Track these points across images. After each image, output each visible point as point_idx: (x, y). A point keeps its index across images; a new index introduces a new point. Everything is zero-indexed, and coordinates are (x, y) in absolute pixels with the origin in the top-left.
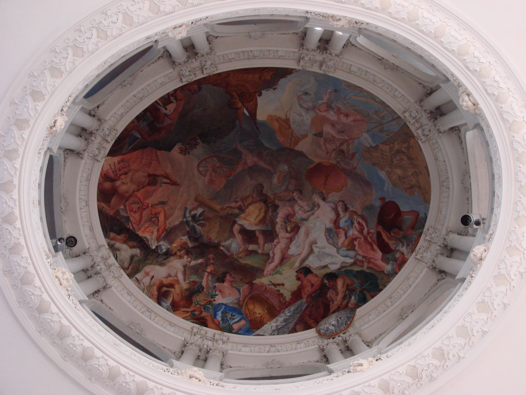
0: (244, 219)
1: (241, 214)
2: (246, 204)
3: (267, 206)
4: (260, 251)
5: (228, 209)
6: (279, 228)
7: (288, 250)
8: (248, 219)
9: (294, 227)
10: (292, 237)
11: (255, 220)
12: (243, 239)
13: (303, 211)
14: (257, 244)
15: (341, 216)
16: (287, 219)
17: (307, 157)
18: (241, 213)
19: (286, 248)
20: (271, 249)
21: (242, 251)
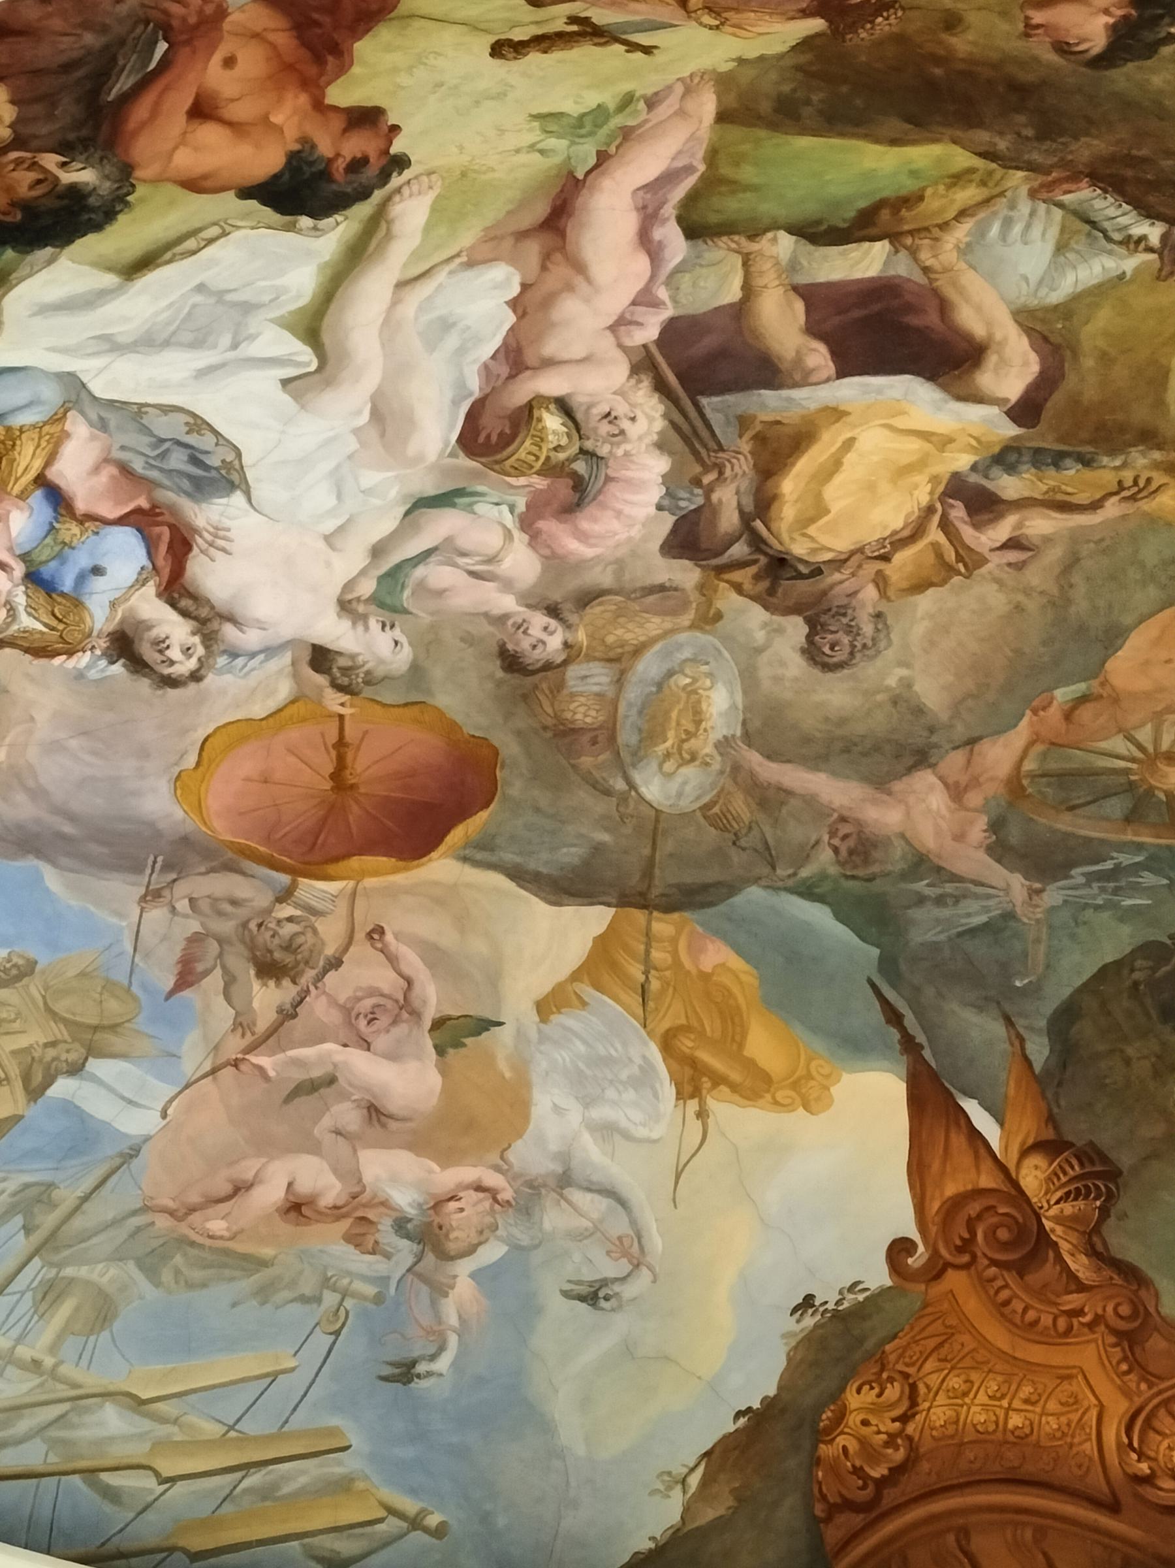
0: (943, 442)
1: (974, 468)
2: (935, 534)
3: (757, 543)
4: (784, 244)
5: (1083, 498)
6: (633, 419)
7: (525, 287)
8: (915, 445)
9: (507, 440)
10: (512, 377)
11: (849, 444)
12: (944, 307)
13: (464, 554)
14: (810, 294)
15: (150, 589)
16: (579, 485)
17: (518, 875)
18: (974, 478)
19: (548, 301)
20: (678, 270)
21: (944, 226)
